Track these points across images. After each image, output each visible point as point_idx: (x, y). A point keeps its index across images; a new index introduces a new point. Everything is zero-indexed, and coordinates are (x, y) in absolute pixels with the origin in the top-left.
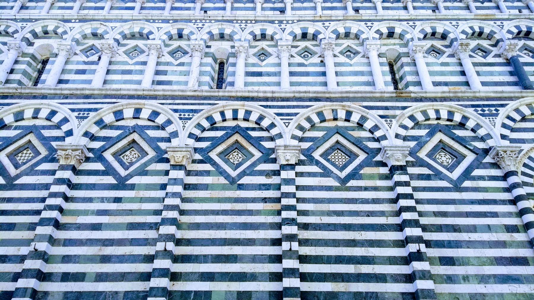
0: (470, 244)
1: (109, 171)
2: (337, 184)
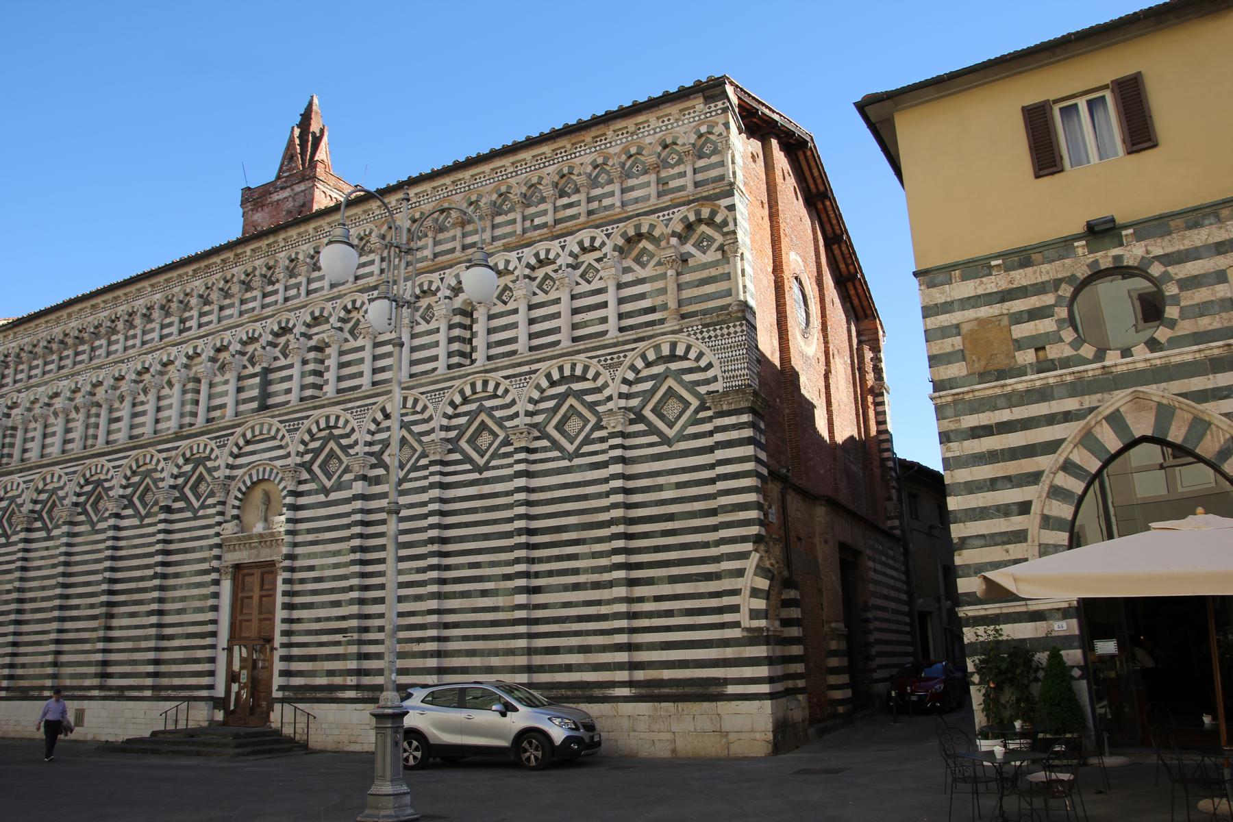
1: (45, 527)
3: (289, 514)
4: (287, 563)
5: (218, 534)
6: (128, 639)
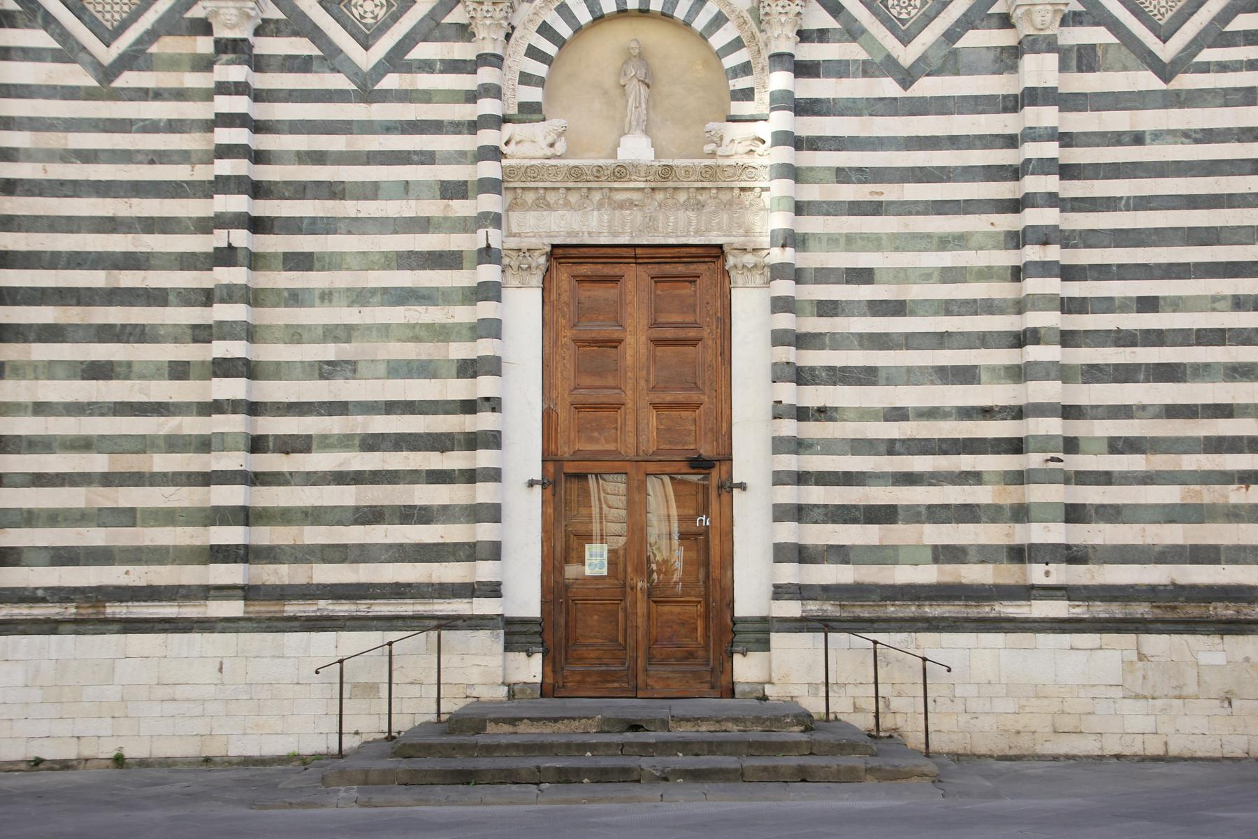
0: (356, 225)
2: (93, 83)
3: (783, 120)
4: (779, 255)
5: (494, 153)
6: (84, 444)
